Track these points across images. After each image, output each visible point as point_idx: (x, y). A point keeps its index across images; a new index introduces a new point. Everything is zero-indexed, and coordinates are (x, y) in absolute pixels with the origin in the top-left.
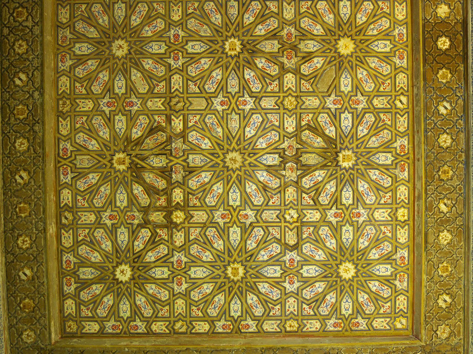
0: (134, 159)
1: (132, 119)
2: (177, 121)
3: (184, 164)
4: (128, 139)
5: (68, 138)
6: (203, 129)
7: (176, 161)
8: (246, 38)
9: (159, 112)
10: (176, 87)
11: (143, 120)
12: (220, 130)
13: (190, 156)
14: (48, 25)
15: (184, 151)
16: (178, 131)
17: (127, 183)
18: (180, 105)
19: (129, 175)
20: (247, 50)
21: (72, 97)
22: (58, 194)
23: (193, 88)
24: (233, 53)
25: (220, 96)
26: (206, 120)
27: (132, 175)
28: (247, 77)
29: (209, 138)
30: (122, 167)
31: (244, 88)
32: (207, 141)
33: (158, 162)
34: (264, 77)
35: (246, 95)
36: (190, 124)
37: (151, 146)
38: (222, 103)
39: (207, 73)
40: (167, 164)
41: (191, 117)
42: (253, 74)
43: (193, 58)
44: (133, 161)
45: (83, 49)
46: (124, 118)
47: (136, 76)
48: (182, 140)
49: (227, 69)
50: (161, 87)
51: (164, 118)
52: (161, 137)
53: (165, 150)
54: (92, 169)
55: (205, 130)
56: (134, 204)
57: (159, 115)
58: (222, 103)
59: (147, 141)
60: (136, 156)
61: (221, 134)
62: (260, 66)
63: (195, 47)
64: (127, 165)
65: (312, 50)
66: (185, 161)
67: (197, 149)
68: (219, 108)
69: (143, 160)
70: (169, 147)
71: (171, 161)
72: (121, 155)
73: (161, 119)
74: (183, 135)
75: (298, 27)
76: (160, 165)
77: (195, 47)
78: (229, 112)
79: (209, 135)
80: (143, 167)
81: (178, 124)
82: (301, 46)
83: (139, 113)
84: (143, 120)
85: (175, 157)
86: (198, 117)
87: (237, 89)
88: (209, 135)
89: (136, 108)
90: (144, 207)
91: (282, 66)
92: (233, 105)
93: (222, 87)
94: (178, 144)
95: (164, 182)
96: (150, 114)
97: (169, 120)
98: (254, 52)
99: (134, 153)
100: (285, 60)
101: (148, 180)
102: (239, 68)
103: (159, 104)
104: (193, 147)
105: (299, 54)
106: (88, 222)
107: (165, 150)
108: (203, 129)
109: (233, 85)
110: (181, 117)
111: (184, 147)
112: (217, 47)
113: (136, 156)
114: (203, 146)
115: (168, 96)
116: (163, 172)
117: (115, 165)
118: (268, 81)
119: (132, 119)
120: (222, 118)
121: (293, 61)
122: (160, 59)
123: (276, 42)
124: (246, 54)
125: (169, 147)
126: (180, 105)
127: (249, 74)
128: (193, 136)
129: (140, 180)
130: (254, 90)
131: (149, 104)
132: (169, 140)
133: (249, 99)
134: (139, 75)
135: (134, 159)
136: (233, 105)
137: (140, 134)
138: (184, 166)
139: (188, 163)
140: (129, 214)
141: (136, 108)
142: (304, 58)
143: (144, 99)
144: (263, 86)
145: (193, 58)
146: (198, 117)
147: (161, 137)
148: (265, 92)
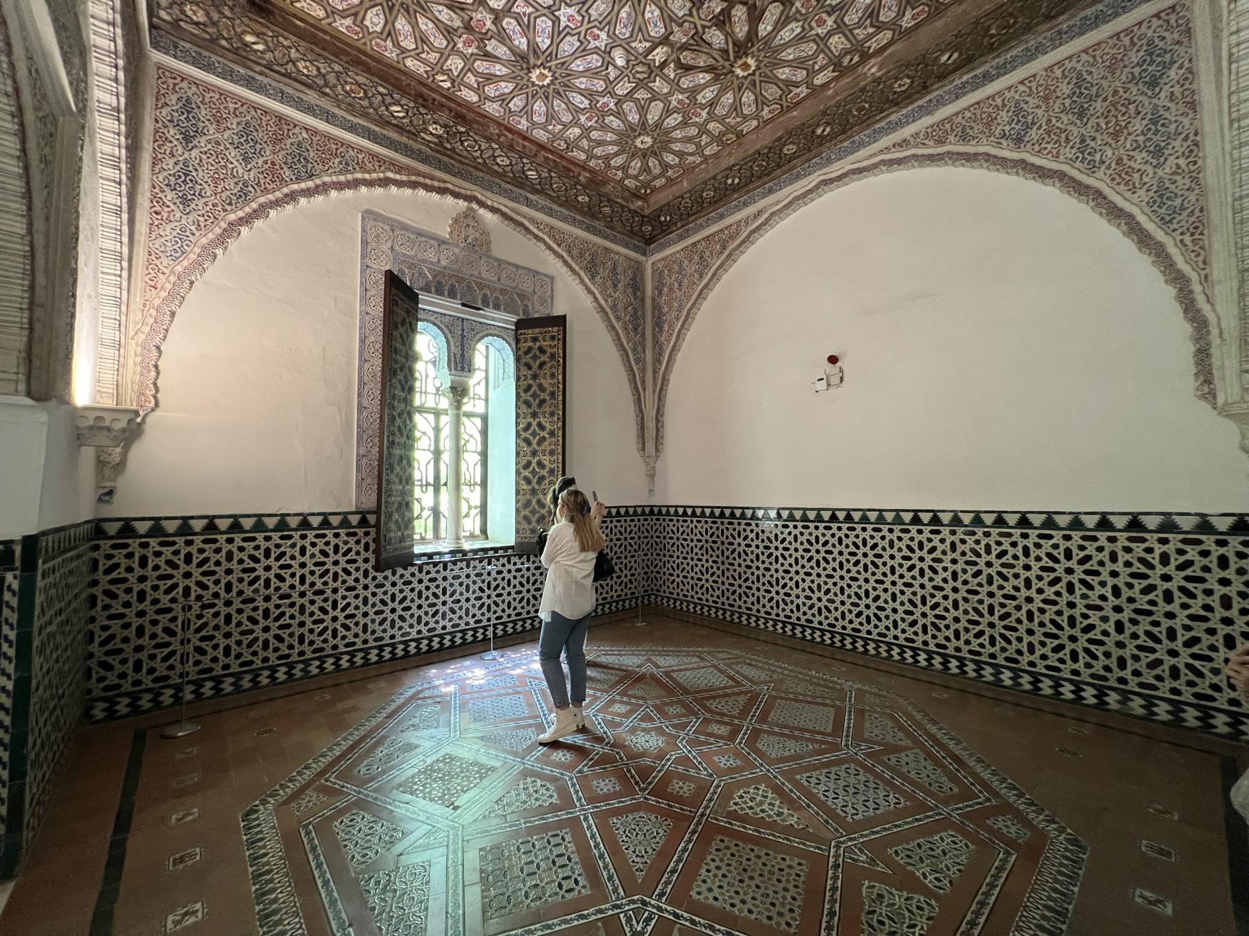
0: (732, 58)
1: (693, 92)
2: (657, 58)
3: (695, 12)
4: (716, 79)
5: (757, 117)
6: (640, 30)
7: (699, 23)
8: (521, 73)
9: (665, 78)
10: (627, 85)
11: (685, 83)
12: (623, 14)
13: (680, 15)
14: (676, 190)
15: (681, 25)
16: (665, 49)
17: (765, 43)
18: (638, 69)
19: (754, 49)
20: (528, 63)
21: (718, 139)
22: (825, 86)
23: (613, 73)
24: (546, 72)
25: (591, 45)
26: (628, 35)
27: (753, 45)
28: (548, 42)
29: (643, 14)
30: (751, 61)
31: (559, 33)
32: (648, 15)
33: (716, 37)
34: (528, 26)
35: (563, 24)
36: (648, 45)
37: (704, 57)
38: (597, 37)
39: (587, 74)
40: (710, 27)
41: (641, 50)
42: (539, 40)
43: (590, 94)
44: (735, 58)
45: (670, 159)
46: (699, 97)
47: (652, 118)
48: (671, 37)
49: (563, 64)
50: (642, 95)
51: (666, 71)
52: (686, 57)
53: (698, 42)
54: (776, 81)
55: (640, 28)
56: (787, 17)
57: (668, 76)
58: (597, 37)
59: (702, 64)
60: (728, 60)
61: (626, 8)
62: (524, 40)
63: (580, 101)
64: (744, 59)
65: (446, 10)
66: (691, 15)
67: (665, 15)
68: (603, 35)
69: (727, 52)
70: (691, 42)
71: (704, 27)
72: (739, 72)
73: (670, 72)
74: (665, 40)
75: (452, 45)
76: (717, 33)
77: (580, 101)
78: (596, 23)
79: (640, 18)
80: (735, 44)
81: (659, 54)
82: (457, 23)
83: (682, 91)
84: (685, 83)
85: (696, 27)
86: (633, 45)
87: (568, 38)
88: (640, 18)
89: (680, 97)
90: (783, 4)
91: (497, 20)
92: (585, 26)
93: (583, 51)
94: (679, 37)
95: (733, 12)
96: (675, 85)
97: (664, 65)
98: (522, 58)
99: (727, 64)
100: (489, 24)
101: (746, 29)
102: (550, 54)
103: (657, 83)
104: (667, 21)
105: (467, 18)
106: (843, 39)
107: (698, 42)
108: (640, 30)
109: (569, 45)
110: (650, 57)
111: (676, 28)
112: (558, 87)
113: (728, 60)
114: (657, 12)
115: (641, 84)
116: (724, 22)
117: (753, 68)
118: (526, 20)
119: (693, 92)
120: (609, 23)
121: (479, 16)
122: (619, 114)
123: (488, 48)
124: (532, 61)
125: (691, 42)
126: (638, 69)
127: (544, 42)
128: (657, 31)
129: (752, 35)
130: (550, 23)
131: (665, 91)
132: (684, 47)
133: (562, 18)
134: (649, 117)
135: (732, 58)
136: (585, 26)
137: (701, 75)
138: (698, 10)
139: (690, 10)
140: (804, 11)
141: (680, 97)
142: (463, 9)
143: (665, 99)
144: (536, 18)
145: (590, 94)
146: (633, 45)
147: (686, 57)
148: (537, 10)
